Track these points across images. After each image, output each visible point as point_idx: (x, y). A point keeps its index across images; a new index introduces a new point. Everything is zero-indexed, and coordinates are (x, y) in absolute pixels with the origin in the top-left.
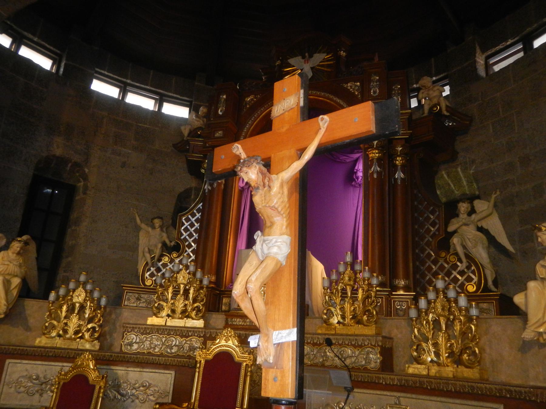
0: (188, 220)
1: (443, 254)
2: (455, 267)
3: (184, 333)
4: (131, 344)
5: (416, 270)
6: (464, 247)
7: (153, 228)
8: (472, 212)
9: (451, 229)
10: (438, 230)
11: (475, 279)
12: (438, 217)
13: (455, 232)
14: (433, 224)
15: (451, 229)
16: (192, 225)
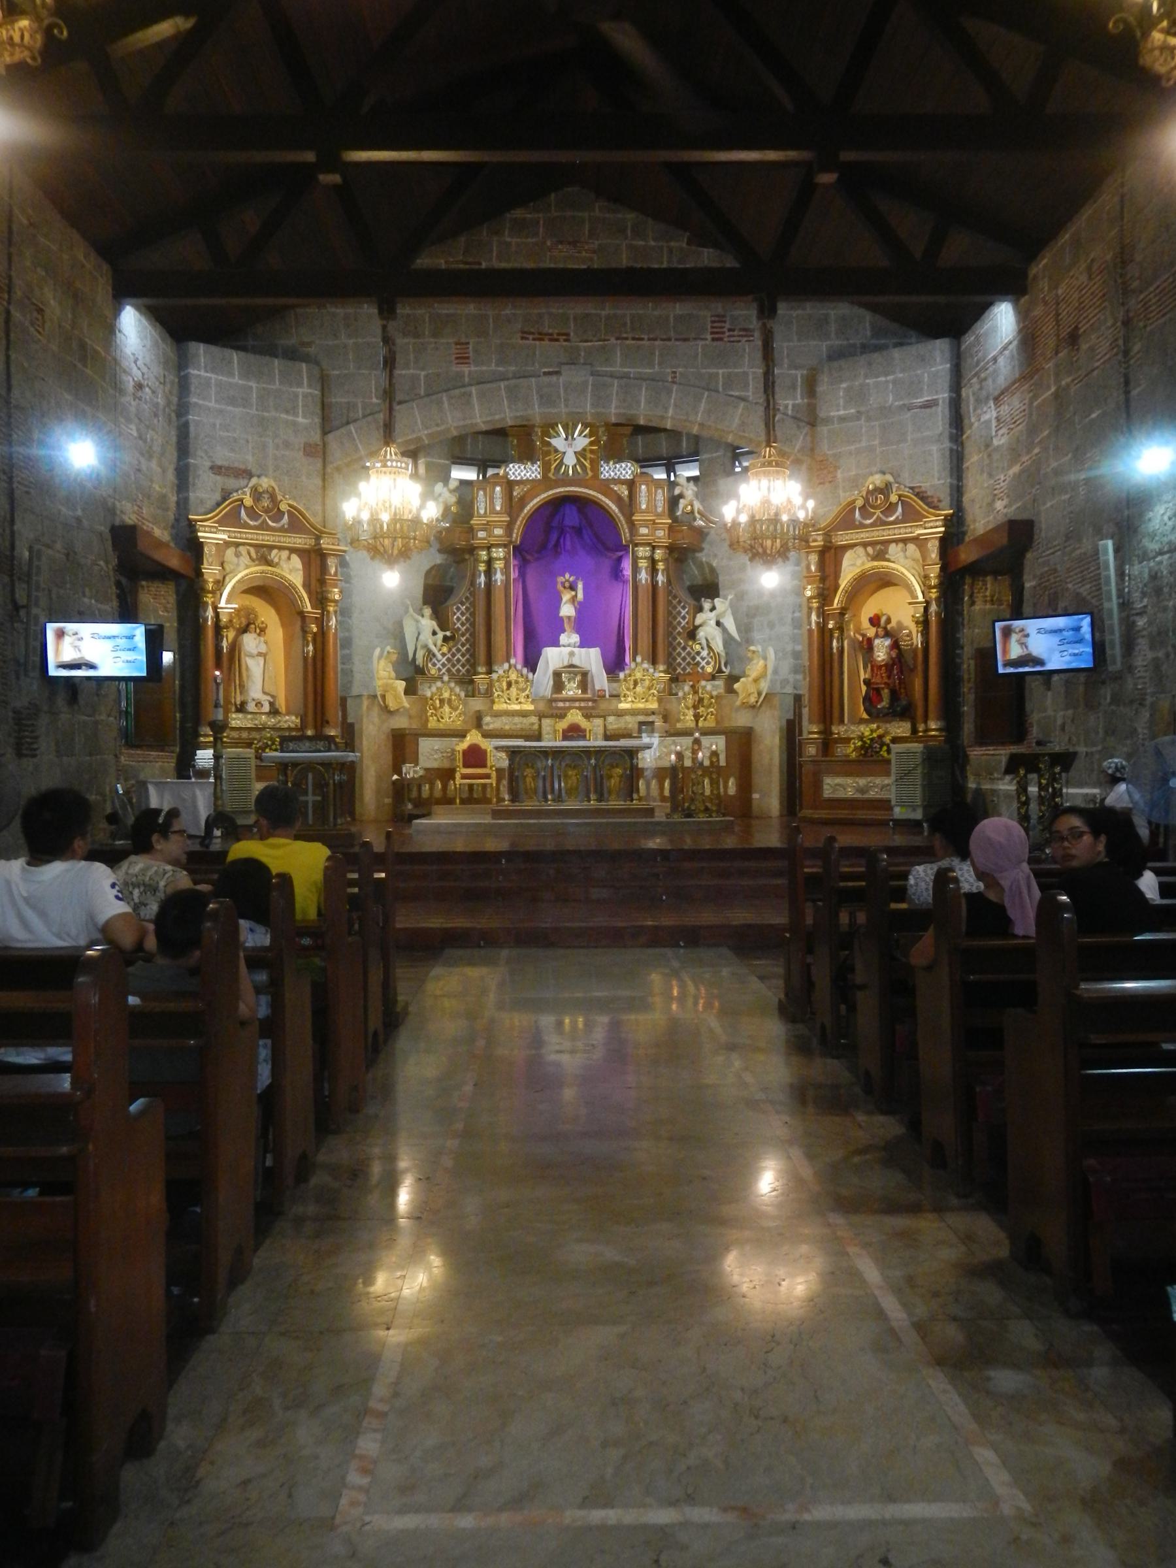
0: (458, 609)
1: (690, 643)
2: (698, 653)
3: (524, 714)
4: (488, 724)
5: (670, 654)
6: (707, 640)
7: (423, 616)
8: (713, 609)
9: (698, 622)
10: (687, 623)
11: (713, 663)
12: (687, 613)
13: (700, 626)
14: (684, 618)
15: (698, 622)
16: (463, 614)
